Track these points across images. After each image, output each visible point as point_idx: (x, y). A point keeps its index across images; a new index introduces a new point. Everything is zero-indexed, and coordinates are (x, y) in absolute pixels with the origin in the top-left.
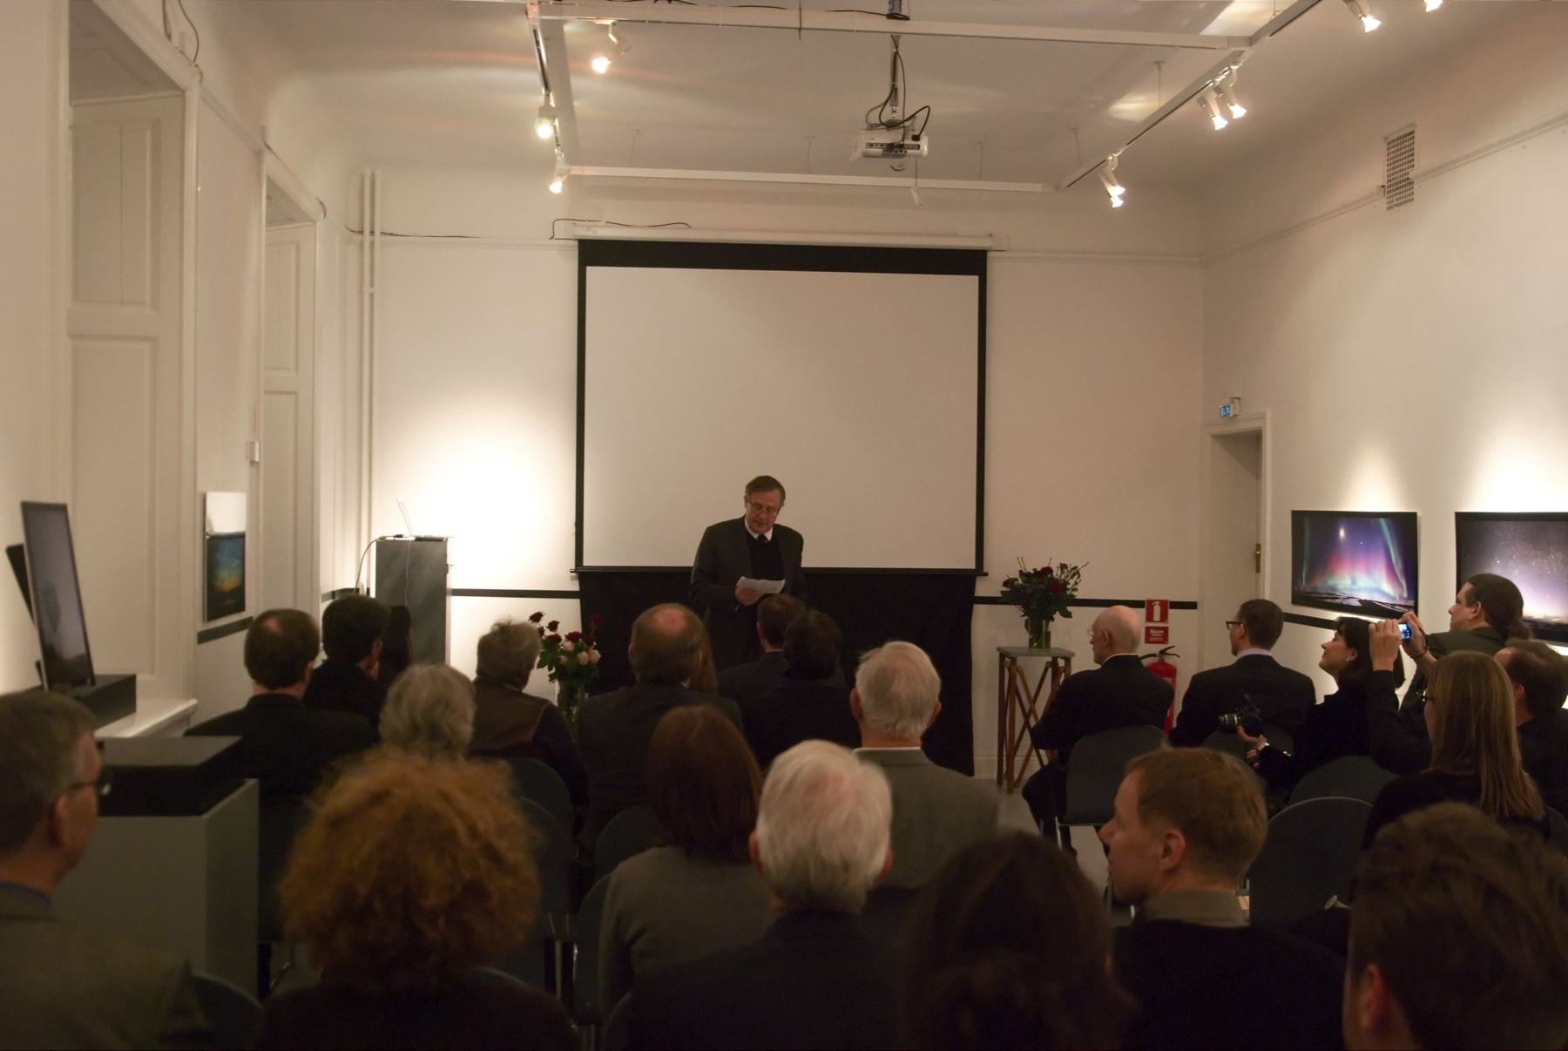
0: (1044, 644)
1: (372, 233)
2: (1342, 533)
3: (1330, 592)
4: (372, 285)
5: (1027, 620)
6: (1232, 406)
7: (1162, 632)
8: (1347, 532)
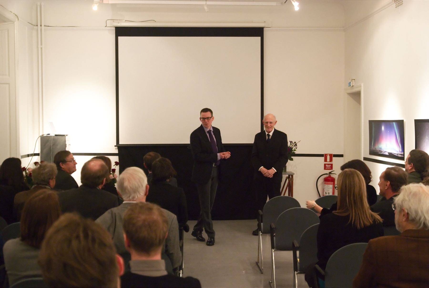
1: (41, 26)
2: (383, 128)
3: (380, 150)
4: (41, 44)
6: (351, 82)
7: (330, 165)
8: (385, 128)
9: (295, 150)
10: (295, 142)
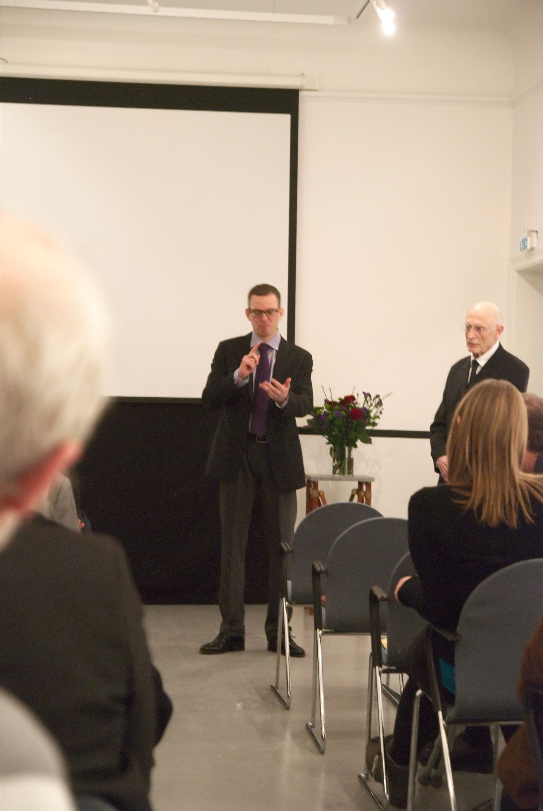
0: (346, 471)
5: (331, 449)
6: (529, 239)
9: (377, 417)
10: (378, 396)
